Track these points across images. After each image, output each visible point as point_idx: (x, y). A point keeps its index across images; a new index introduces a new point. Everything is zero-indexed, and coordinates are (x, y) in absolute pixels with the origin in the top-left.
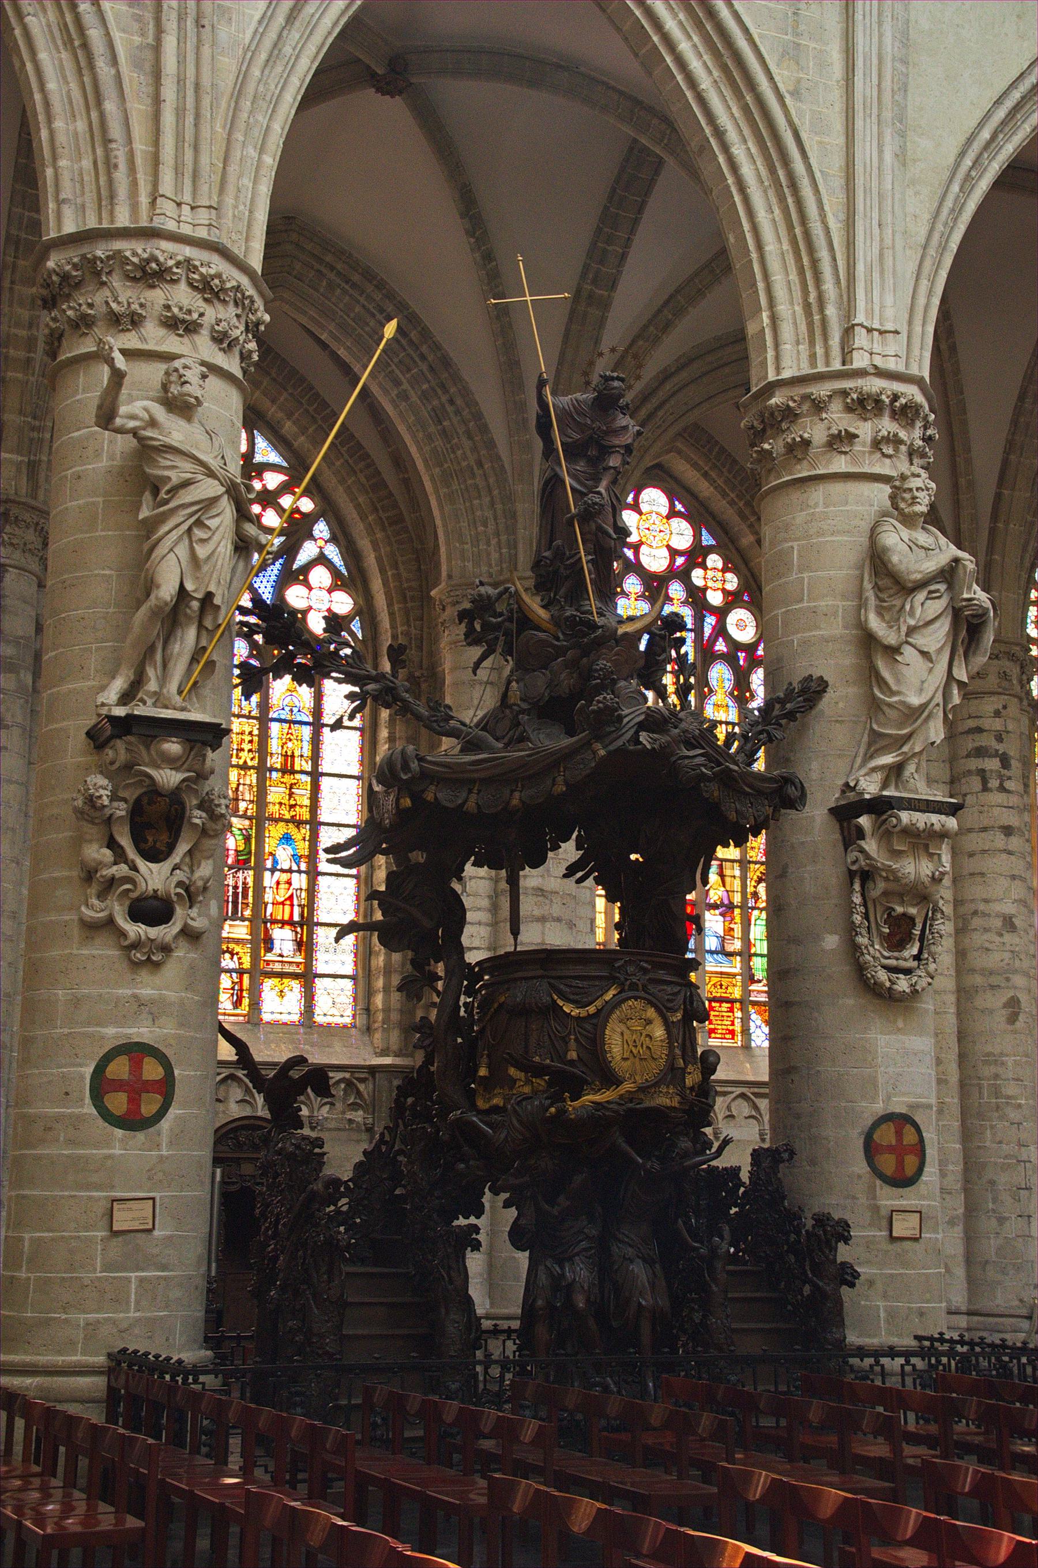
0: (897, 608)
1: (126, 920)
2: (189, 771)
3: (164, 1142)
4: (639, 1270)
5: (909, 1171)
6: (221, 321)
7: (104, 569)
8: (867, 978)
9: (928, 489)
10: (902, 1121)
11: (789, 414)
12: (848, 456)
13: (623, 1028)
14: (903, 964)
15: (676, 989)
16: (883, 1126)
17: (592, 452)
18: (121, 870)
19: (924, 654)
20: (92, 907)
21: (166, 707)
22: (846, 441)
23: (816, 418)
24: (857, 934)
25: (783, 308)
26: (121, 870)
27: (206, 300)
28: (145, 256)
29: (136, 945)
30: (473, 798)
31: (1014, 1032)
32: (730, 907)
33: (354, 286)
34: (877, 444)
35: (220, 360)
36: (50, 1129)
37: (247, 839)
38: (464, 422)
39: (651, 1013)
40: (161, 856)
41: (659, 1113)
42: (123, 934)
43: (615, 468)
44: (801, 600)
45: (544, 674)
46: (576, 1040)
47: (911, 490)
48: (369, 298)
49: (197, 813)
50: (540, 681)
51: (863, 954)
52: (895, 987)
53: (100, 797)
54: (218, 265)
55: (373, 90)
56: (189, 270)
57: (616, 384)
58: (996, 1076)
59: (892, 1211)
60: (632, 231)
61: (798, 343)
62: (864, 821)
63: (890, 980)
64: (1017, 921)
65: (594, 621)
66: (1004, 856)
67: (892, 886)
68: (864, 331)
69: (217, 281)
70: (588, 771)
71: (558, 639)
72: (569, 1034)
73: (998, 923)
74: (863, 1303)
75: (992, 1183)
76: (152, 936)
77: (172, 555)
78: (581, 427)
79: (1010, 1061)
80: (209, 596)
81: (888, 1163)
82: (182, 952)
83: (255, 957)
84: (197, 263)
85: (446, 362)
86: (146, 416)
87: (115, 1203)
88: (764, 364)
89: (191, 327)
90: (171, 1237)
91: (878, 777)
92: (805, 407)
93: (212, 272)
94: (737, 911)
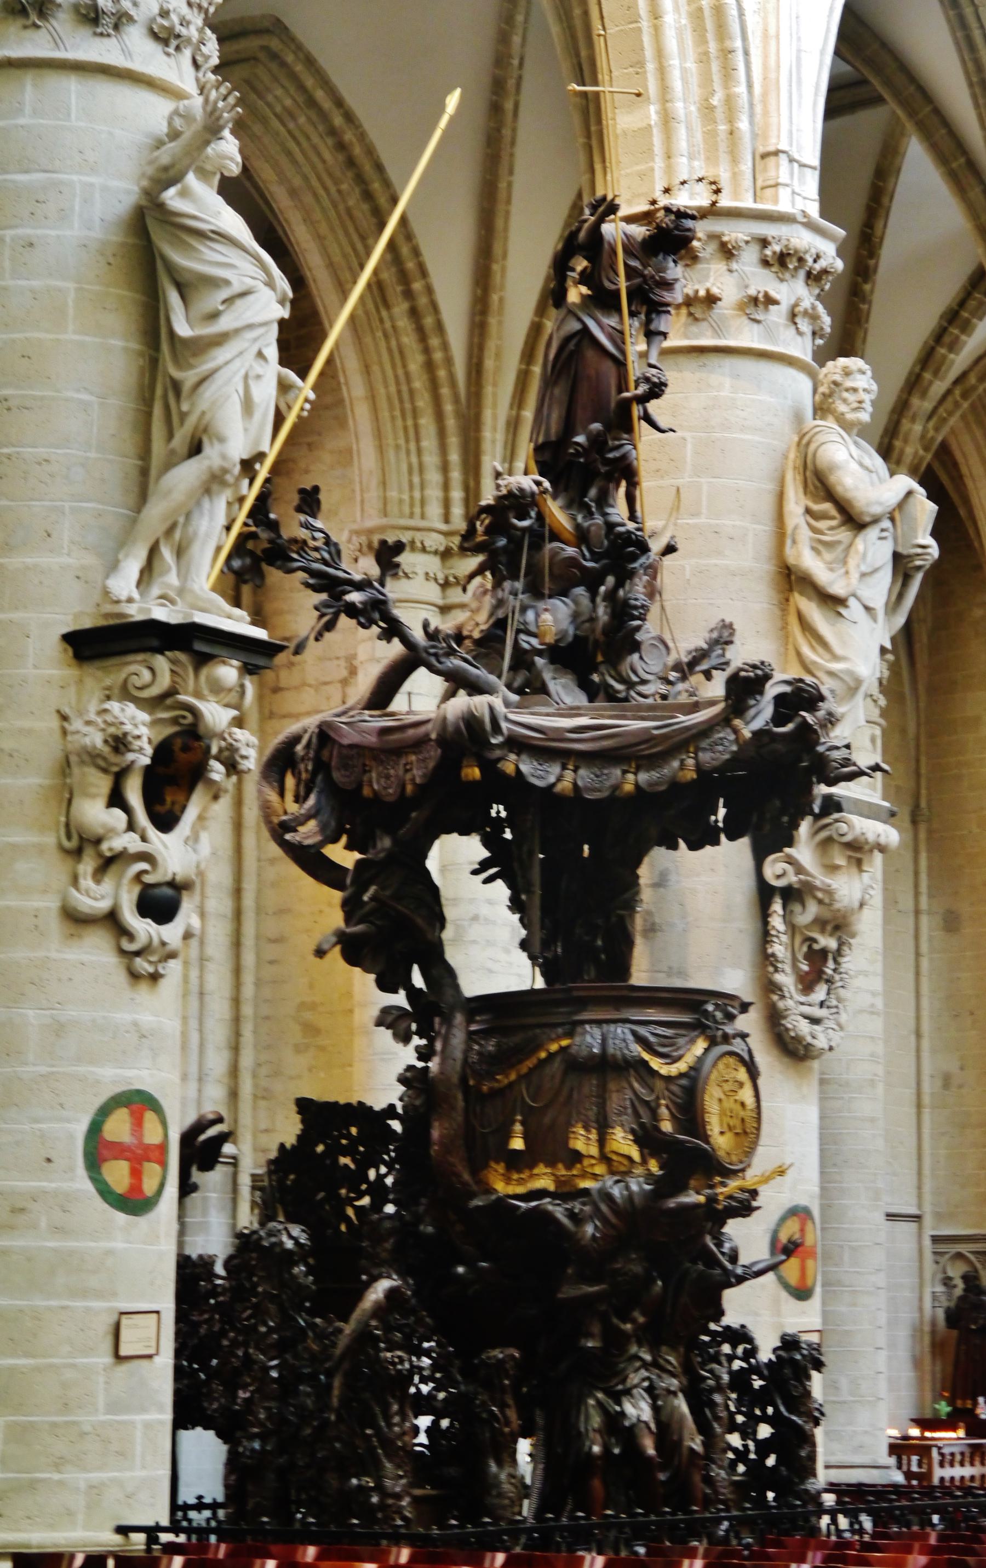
7: (78, 391)
8: (787, 1030)
12: (761, 326)
18: (131, 842)
19: (867, 609)
22: (761, 306)
24: (776, 970)
25: (679, 107)
30: (569, 775)
36: (22, 1210)
44: (696, 514)
45: (563, 602)
47: (855, 390)
51: (783, 997)
53: (139, 737)
70: (727, 756)
72: (658, 1098)
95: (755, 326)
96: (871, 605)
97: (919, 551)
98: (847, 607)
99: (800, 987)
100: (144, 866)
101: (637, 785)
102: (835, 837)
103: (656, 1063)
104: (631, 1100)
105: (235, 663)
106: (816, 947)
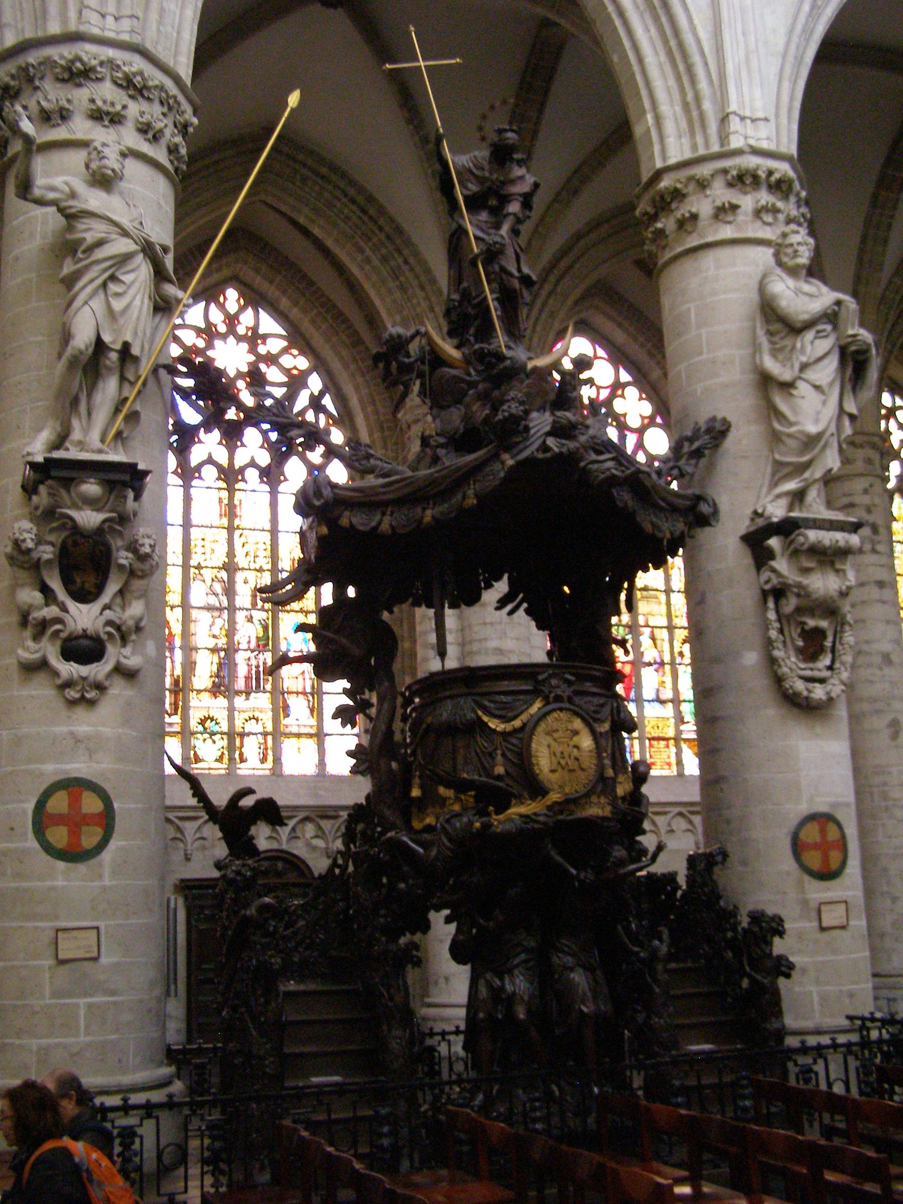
0: (789, 348)
1: (59, 660)
2: (111, 511)
3: (107, 871)
4: (578, 977)
5: (834, 865)
6: (144, 113)
8: (787, 689)
9: (807, 244)
10: (824, 819)
11: (678, 195)
12: (733, 226)
13: (549, 740)
14: (816, 674)
15: (602, 700)
17: (493, 202)
18: (52, 611)
19: (817, 388)
20: (27, 649)
21: (87, 451)
23: (701, 196)
24: (774, 648)
25: (665, 108)
26: (52, 611)
27: (131, 97)
28: (70, 57)
29: (68, 684)
31: (897, 747)
32: (662, 664)
33: (323, 177)
34: (758, 213)
35: (146, 148)
37: (265, 628)
38: (417, 277)
39: (578, 724)
40: (90, 598)
41: (591, 823)
42: (56, 674)
43: (515, 215)
44: (701, 354)
46: (503, 755)
47: (791, 245)
48: (336, 186)
49: (123, 553)
50: (455, 417)
51: (780, 666)
52: (812, 695)
54: (137, 63)
55: (319, 5)
56: (113, 69)
57: (510, 135)
58: (885, 784)
59: (820, 904)
60: (541, 111)
61: (680, 137)
62: (774, 542)
63: (807, 689)
64: (893, 657)
65: (502, 352)
66: (880, 605)
67: (804, 602)
68: (737, 119)
69: (139, 78)
70: (497, 483)
71: (469, 375)
72: (496, 749)
73: (877, 660)
75: (885, 870)
76: (84, 674)
77: (86, 309)
78: (480, 180)
79: (894, 770)
80: (126, 346)
81: (814, 859)
82: (118, 689)
83: (276, 721)
84: (120, 63)
85: (399, 230)
86: (67, 189)
87: (60, 933)
88: (652, 158)
89: (116, 119)
90: (118, 964)
91: (783, 502)
92: (692, 187)
93: (134, 69)
94: (667, 668)
95: (728, 226)
96: (818, 383)
97: (850, 340)
98: (796, 388)
99: (801, 657)
100: (58, 627)
101: (433, 517)
102: (799, 547)
103: (493, 724)
104: (476, 752)
105: (92, 480)
106: (807, 628)
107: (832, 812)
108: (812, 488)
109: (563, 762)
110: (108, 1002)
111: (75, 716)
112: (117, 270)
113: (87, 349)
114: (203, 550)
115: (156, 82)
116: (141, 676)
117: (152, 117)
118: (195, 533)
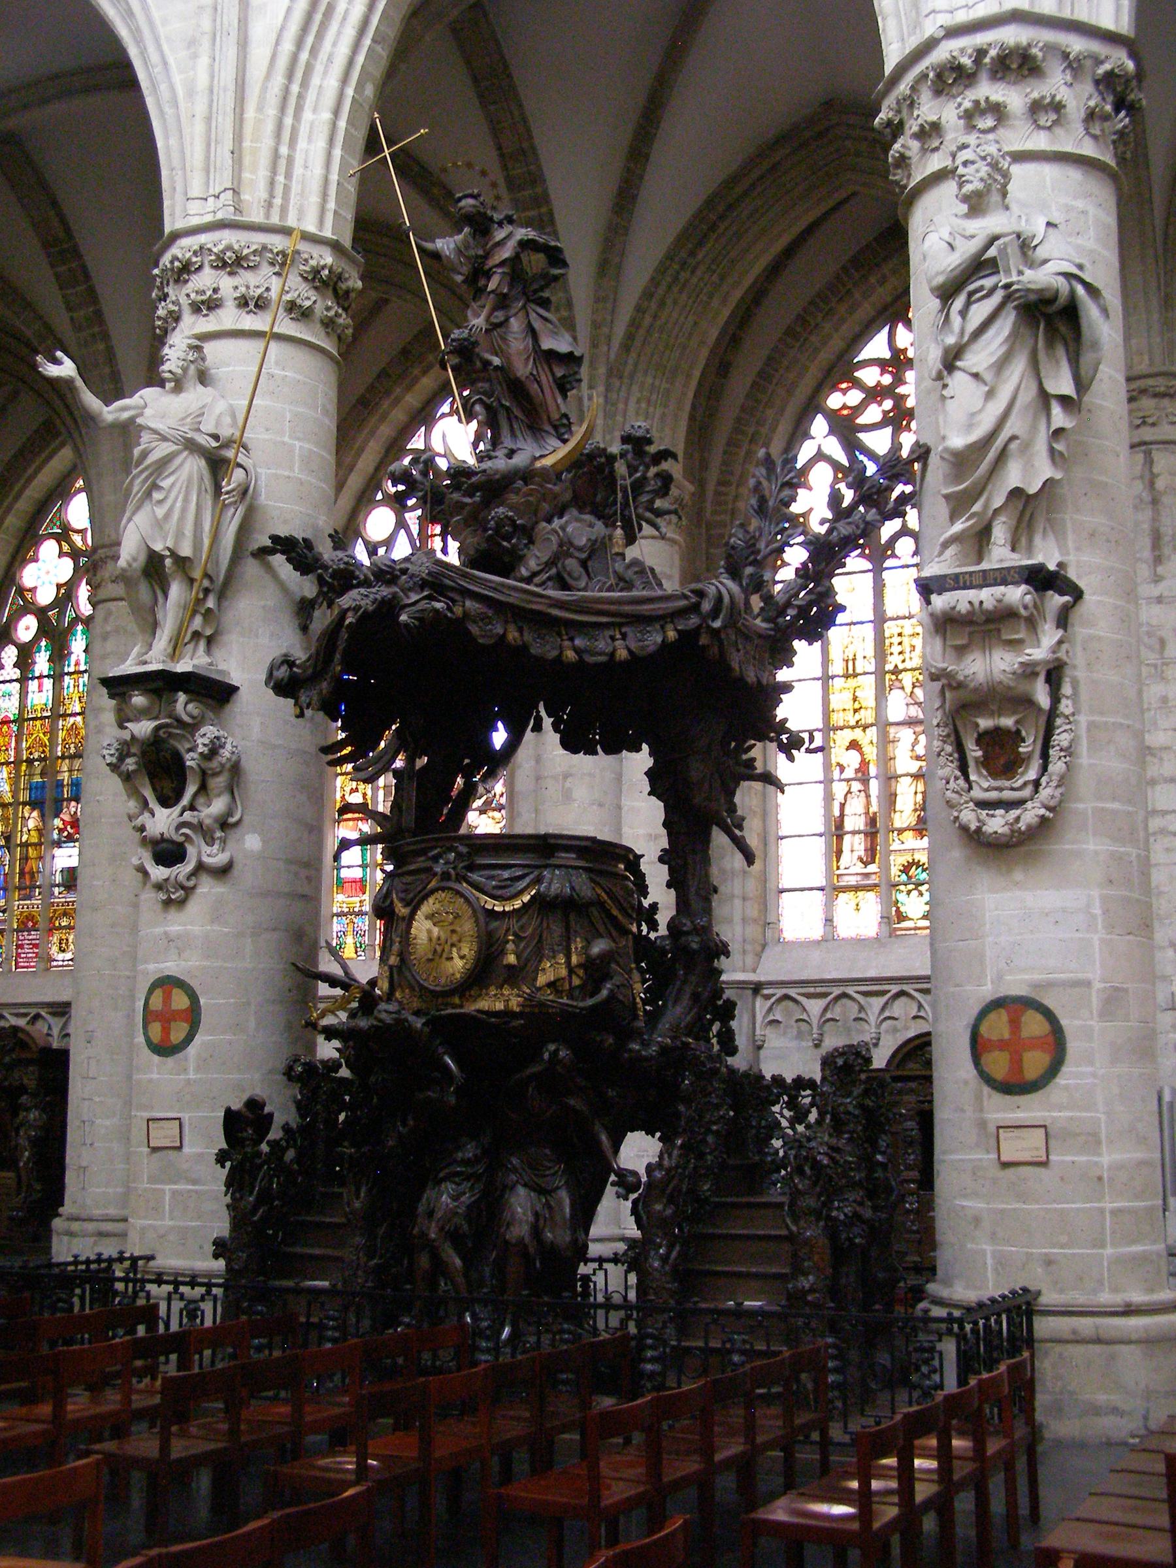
3: (192, 1066)
11: (896, 129)
13: (428, 924)
14: (1007, 795)
16: (992, 1016)
19: (976, 376)
27: (231, 274)
29: (159, 887)
35: (249, 322)
43: (493, 291)
54: (228, 238)
59: (999, 1127)
63: (979, 820)
69: (228, 254)
74: (969, 1246)
77: (131, 525)
81: (998, 1064)
82: (207, 887)
84: (209, 246)
93: (221, 247)
96: (974, 371)
107: (1033, 995)
108: (995, 523)
109: (439, 949)
110: (189, 1191)
111: (169, 917)
112: (158, 477)
113: (130, 565)
114: (899, 649)
115: (253, 248)
116: (236, 871)
117: (248, 287)
118: (890, 628)
